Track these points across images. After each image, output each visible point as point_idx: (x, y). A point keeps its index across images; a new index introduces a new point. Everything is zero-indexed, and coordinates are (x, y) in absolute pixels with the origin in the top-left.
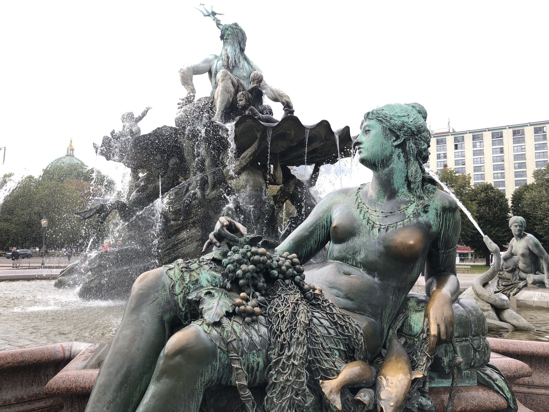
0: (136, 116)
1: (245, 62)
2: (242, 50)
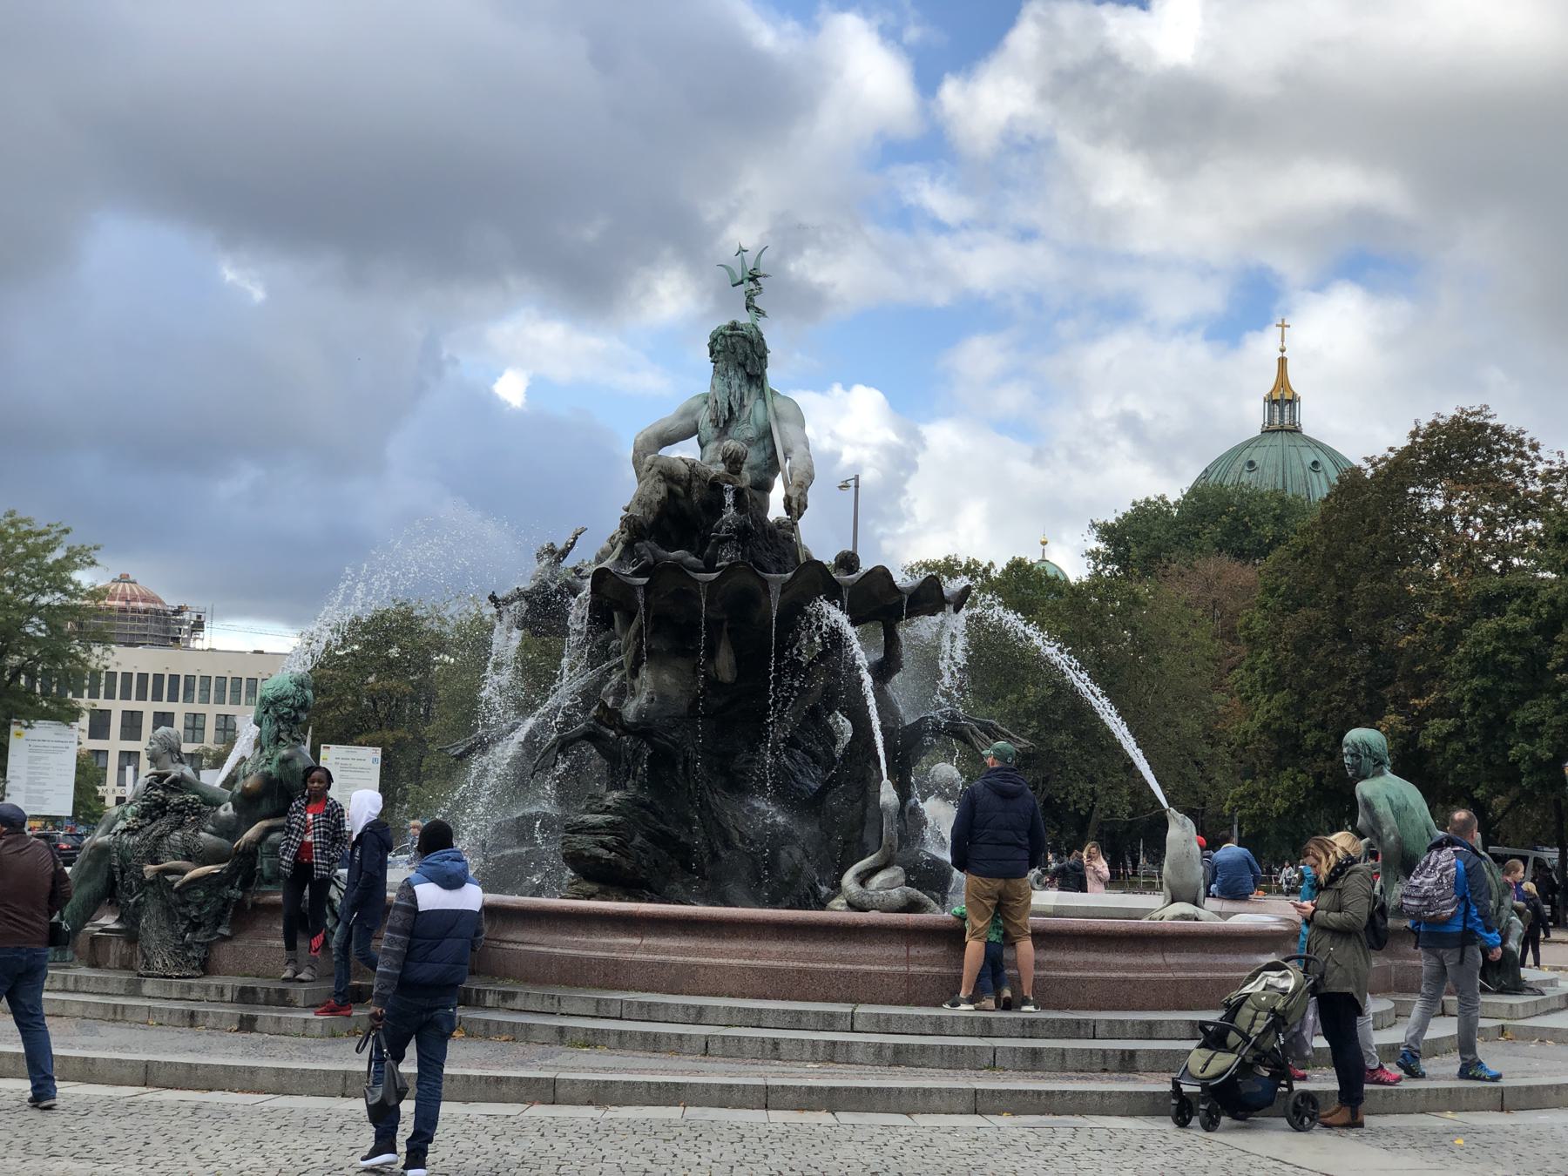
0: (560, 546)
1: (760, 402)
2: (756, 379)
